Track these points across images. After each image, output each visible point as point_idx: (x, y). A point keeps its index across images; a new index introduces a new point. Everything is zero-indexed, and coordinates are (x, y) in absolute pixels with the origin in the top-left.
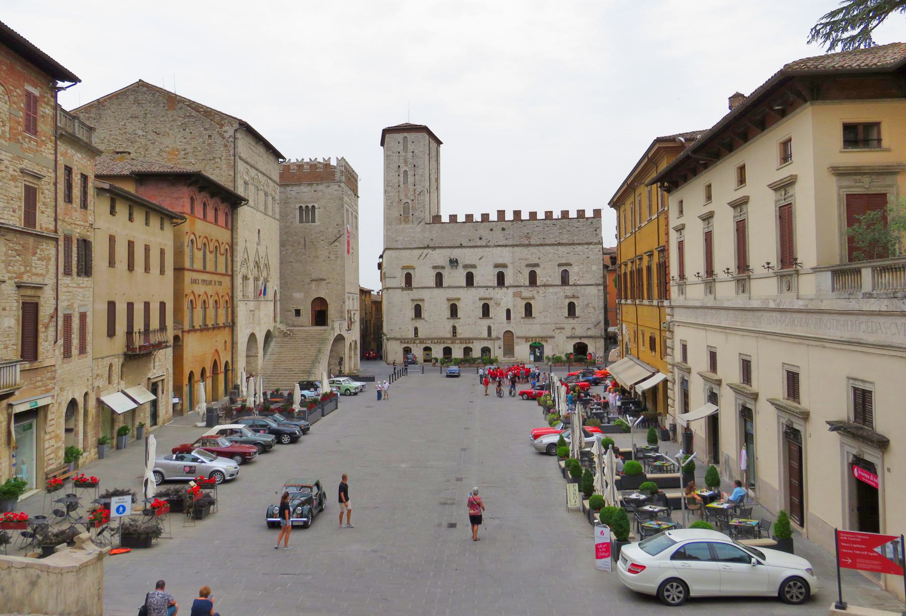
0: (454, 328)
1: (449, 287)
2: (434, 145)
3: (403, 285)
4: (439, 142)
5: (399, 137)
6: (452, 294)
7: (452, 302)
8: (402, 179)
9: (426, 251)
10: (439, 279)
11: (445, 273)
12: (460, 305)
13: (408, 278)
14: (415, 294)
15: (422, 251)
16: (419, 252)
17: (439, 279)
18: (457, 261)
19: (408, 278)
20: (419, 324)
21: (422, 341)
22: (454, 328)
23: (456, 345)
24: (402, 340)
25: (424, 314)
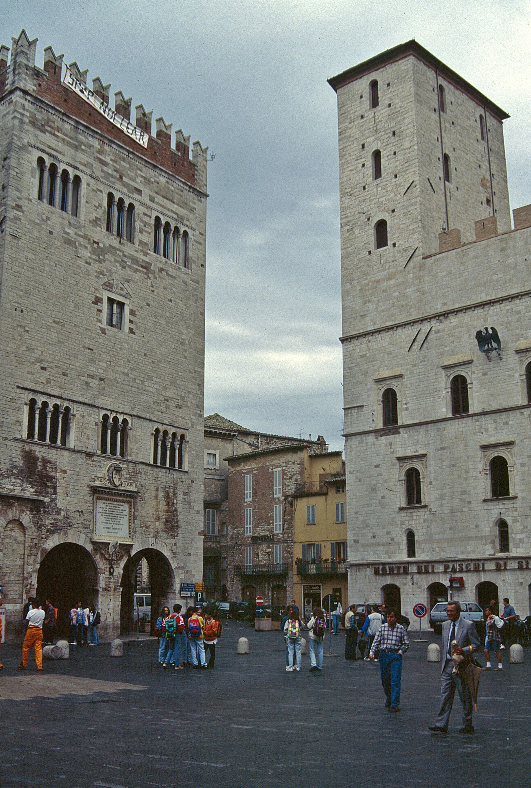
0: (503, 525)
1: (484, 413)
2: (491, 122)
3: (380, 425)
4: (501, 115)
5: (362, 85)
6: (493, 432)
7: (494, 454)
8: (370, 170)
9: (426, 327)
10: (459, 389)
11: (472, 376)
12: (514, 460)
13: (390, 400)
14: (404, 444)
15: (417, 327)
16: (411, 331)
17: (459, 389)
18: (495, 336)
19: (390, 400)
20: (417, 521)
21: (425, 568)
22: (503, 525)
23: (509, 577)
24: (380, 569)
25: (428, 494)
